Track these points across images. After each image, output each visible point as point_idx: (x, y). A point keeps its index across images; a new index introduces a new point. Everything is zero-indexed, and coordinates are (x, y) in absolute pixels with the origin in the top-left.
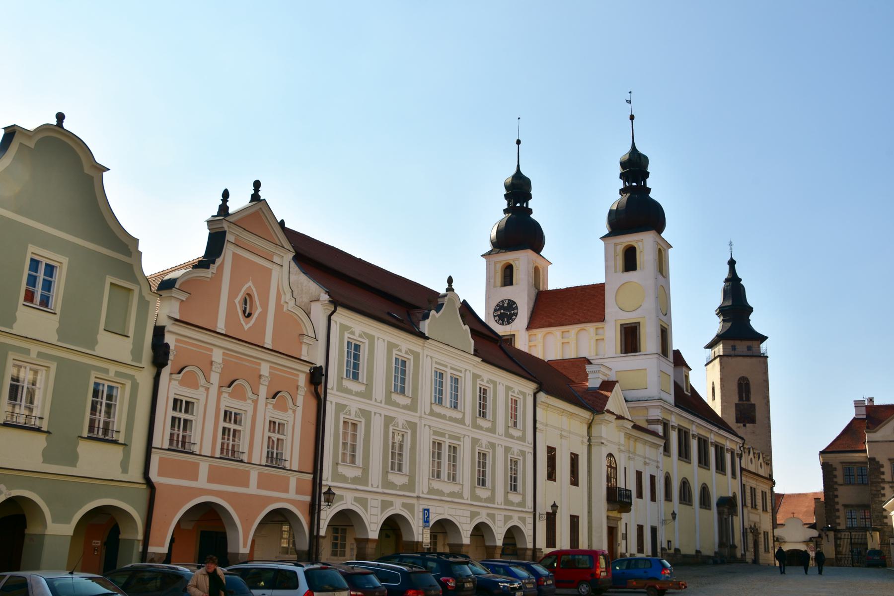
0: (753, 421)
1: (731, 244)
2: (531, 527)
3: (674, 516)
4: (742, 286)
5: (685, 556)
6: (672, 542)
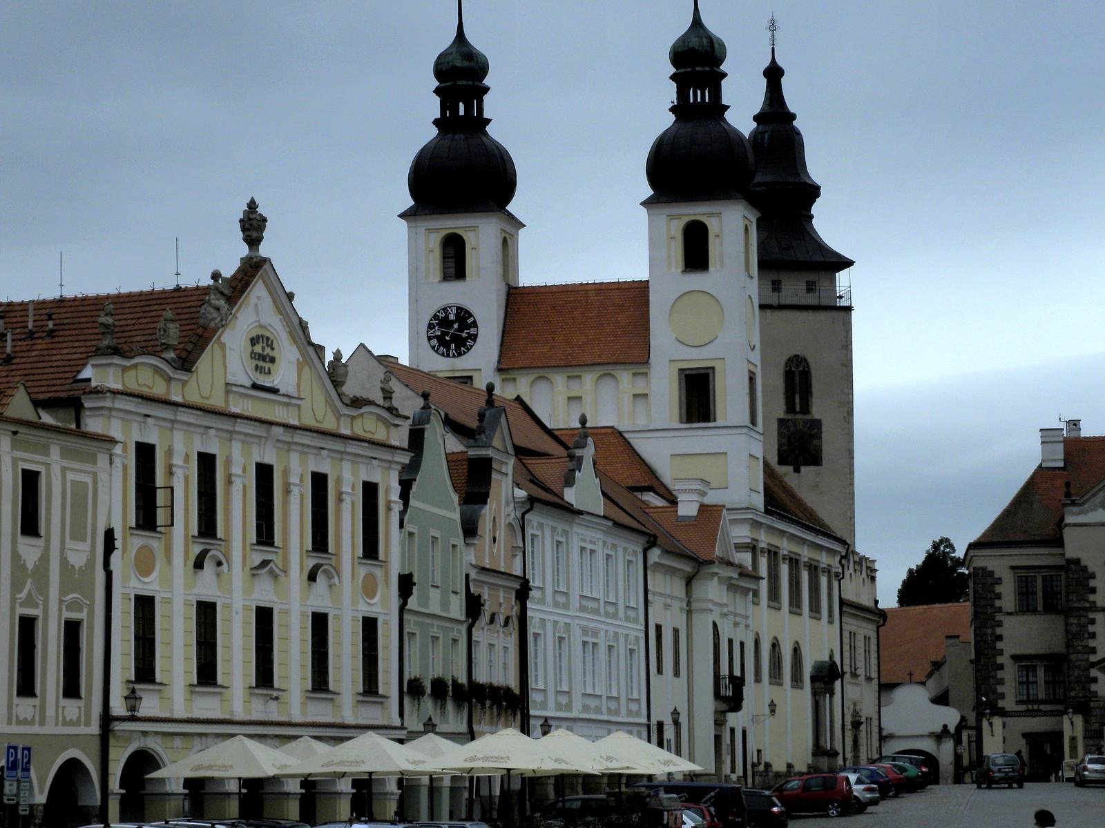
0: (815, 459)
1: (773, 27)
4: (799, 134)
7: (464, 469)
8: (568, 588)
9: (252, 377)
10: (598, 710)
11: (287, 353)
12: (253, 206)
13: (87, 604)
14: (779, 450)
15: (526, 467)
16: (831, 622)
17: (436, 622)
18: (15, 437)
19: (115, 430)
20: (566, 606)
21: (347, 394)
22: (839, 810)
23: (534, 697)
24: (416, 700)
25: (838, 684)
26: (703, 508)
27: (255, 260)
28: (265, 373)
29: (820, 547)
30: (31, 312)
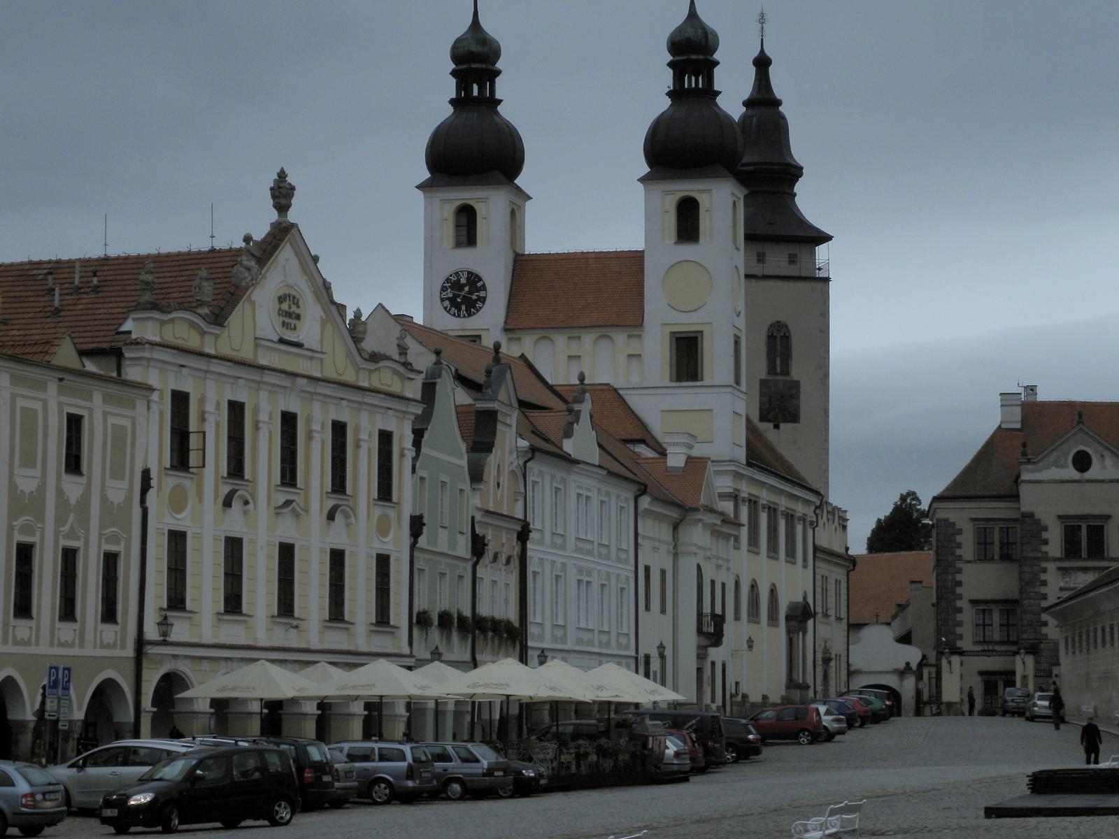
0: (794, 418)
1: (762, 19)
4: (784, 118)
6: (740, 684)
7: (472, 420)
8: (565, 530)
9: (279, 332)
10: (590, 642)
11: (312, 312)
12: (283, 176)
13: (125, 538)
14: (760, 409)
15: (528, 419)
16: (805, 566)
17: (444, 560)
18: (62, 384)
19: (153, 379)
20: (563, 547)
21: (366, 349)
22: (809, 738)
23: (532, 630)
24: (425, 631)
25: (810, 623)
26: (690, 460)
27: (284, 225)
28: (291, 329)
29: (797, 498)
30: (77, 269)
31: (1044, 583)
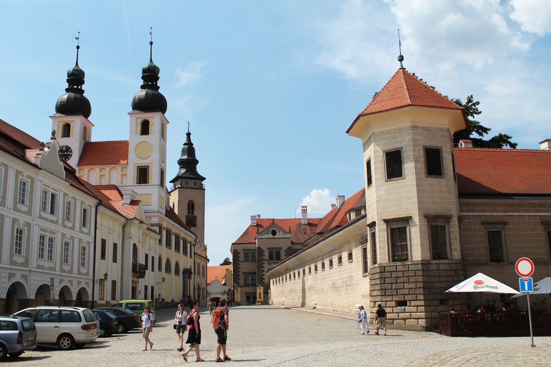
0: (195, 225)
1: (189, 123)
2: (91, 288)
3: (164, 279)
5: (167, 303)
31: (264, 267)
